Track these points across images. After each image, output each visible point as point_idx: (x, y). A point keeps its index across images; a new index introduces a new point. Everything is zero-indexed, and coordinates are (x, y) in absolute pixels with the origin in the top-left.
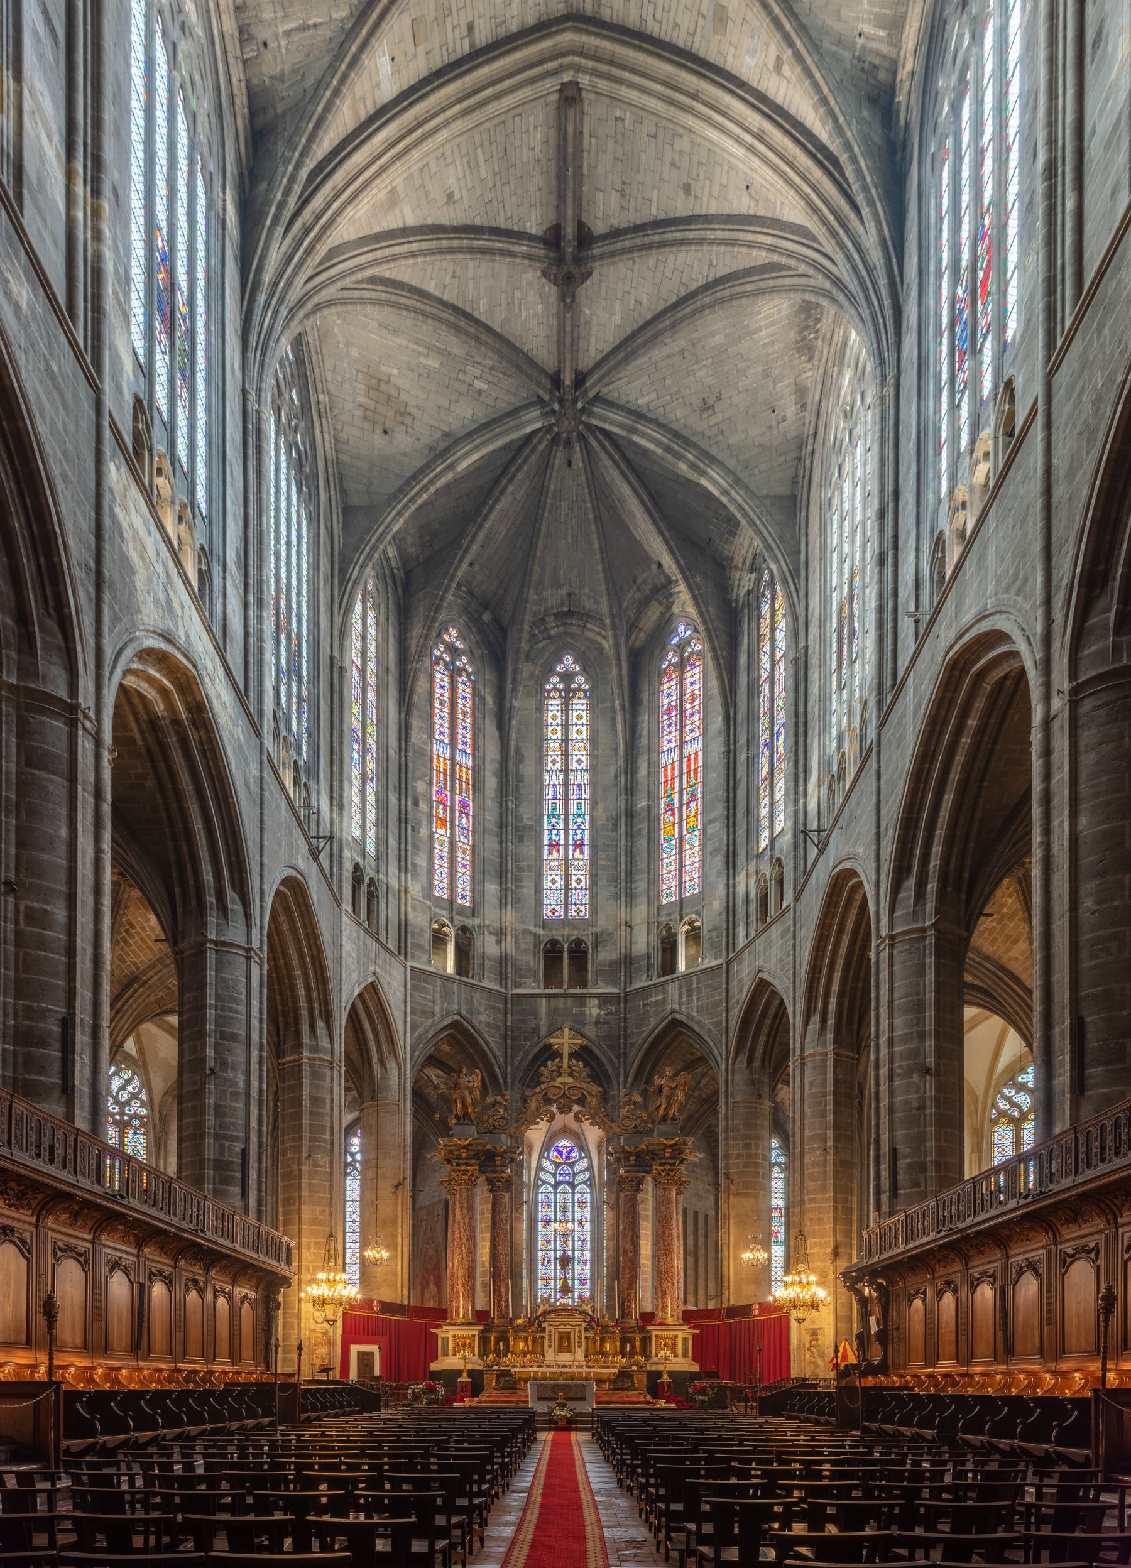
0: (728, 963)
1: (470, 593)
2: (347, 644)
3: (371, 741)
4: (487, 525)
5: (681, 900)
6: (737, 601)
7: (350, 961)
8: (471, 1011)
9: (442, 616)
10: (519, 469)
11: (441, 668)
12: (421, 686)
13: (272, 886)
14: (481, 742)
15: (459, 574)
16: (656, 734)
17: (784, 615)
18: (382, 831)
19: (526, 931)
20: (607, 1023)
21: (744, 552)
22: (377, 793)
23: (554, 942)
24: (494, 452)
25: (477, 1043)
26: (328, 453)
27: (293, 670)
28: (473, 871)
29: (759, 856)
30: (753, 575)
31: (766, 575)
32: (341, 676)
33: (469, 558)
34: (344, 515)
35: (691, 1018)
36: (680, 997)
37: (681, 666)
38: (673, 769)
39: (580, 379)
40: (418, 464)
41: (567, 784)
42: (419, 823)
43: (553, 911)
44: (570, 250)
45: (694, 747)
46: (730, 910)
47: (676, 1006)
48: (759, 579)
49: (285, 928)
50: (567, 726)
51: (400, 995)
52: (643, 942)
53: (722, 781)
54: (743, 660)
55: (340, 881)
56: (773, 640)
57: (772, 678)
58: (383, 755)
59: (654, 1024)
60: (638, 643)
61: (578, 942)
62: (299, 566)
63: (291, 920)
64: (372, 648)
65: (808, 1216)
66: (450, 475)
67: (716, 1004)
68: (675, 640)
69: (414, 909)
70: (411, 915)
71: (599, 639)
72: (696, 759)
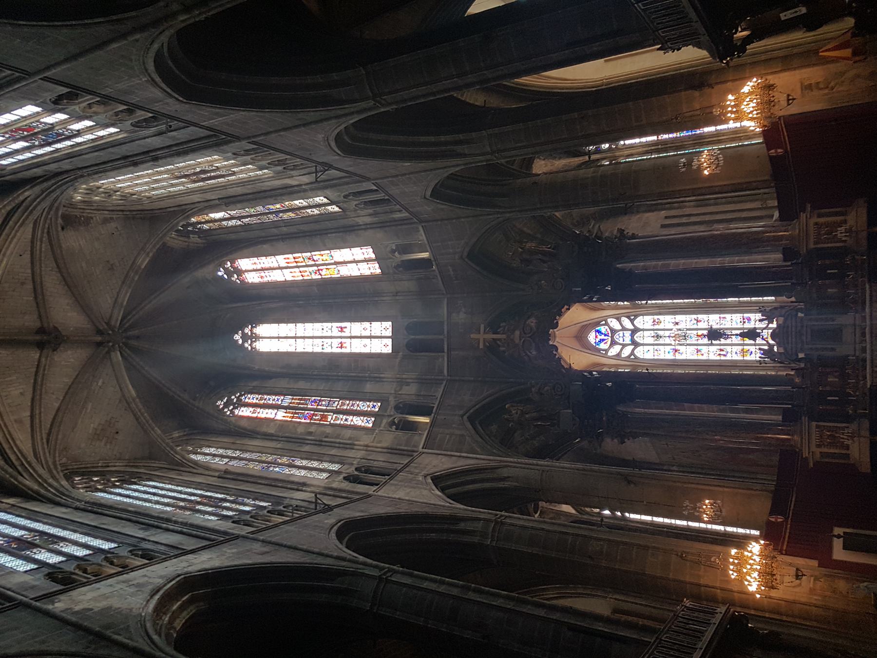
2: (214, 466)
3: (270, 458)
17: (207, 215)
22: (302, 459)
26: (124, 464)
39: (100, 332)
44: (45, 338)
46: (381, 225)
47: (457, 257)
57: (239, 218)
64: (221, 451)
66: (137, 400)
69: (380, 442)
70: (385, 445)
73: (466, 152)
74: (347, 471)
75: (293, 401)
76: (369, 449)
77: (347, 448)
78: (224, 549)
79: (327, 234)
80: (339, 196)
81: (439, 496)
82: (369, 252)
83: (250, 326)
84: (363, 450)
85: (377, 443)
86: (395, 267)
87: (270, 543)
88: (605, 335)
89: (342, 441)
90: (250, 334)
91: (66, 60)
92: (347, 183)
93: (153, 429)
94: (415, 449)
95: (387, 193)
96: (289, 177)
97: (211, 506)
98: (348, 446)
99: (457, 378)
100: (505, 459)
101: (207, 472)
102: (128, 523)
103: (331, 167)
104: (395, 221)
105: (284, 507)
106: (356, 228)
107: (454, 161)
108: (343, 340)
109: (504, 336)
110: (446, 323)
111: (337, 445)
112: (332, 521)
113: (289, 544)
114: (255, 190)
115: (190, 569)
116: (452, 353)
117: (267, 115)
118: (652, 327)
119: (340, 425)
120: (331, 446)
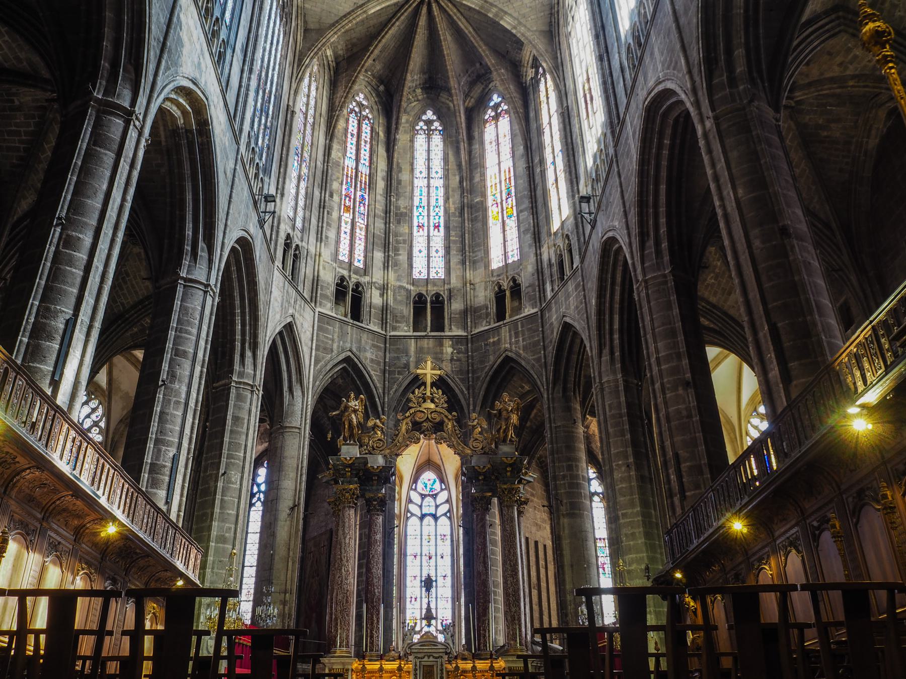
0: (542, 311)
1: (373, 75)
3: (306, 155)
4: (384, 41)
5: (507, 265)
6: (526, 83)
7: (276, 304)
8: (359, 349)
9: (356, 87)
10: (403, 14)
11: (354, 114)
12: (341, 124)
13: (230, 243)
14: (375, 159)
15: (367, 64)
16: (482, 156)
18: (308, 214)
19: (401, 287)
20: (459, 360)
21: (527, 58)
23: (420, 295)
24: (388, 6)
25: (363, 376)
27: (264, 110)
28: (366, 243)
29: (555, 234)
30: (534, 70)
31: (541, 70)
32: (292, 116)
33: (373, 57)
34: (304, 33)
35: (519, 355)
36: (510, 339)
37: (496, 118)
38: (496, 178)
40: (348, 10)
41: (429, 187)
42: (332, 208)
43: (420, 273)
45: (507, 163)
46: (539, 271)
47: (508, 346)
48: (537, 73)
49: (234, 276)
50: (429, 151)
51: (309, 334)
52: (483, 296)
53: (527, 185)
54: (532, 114)
55: (276, 245)
56: (548, 103)
57: (550, 124)
58: (313, 164)
59: (493, 360)
60: (470, 104)
61: (437, 295)
62: (276, 56)
63: (239, 270)
64: (312, 102)
65: (624, 531)
66: (365, 16)
67: (536, 344)
68: (492, 104)
69: (324, 268)
71: (448, 102)
72: (509, 171)
73: (603, 359)
74: (295, 237)
75: (364, 176)
76: (317, 257)
77: (317, 234)
78: (228, 134)
79: (533, 214)
80: (568, 230)
81: (274, 331)
82: (514, 256)
83: (440, 128)
84: (316, 251)
85: (323, 265)
86: (498, 283)
87: (234, 176)
88: (431, 489)
89: (324, 229)
90: (433, 128)
91: (674, 11)
92: (579, 240)
93: (335, 33)
94: (318, 304)
95: (569, 279)
96: (586, 182)
97: (262, 105)
98: (319, 236)
99: (388, 345)
100: (310, 393)
101: (292, 92)
102: (247, 30)
103: (593, 227)
104: (543, 285)
105: (262, 178)
106: (538, 244)
107: (595, 344)
108: (426, 228)
109: (428, 394)
110: (442, 334)
111: (320, 225)
112: (252, 230)
113: (234, 195)
114: (575, 146)
115: (212, 107)
116: (413, 340)
117: (633, 178)
118: (438, 534)
119: (339, 227)
120: (319, 218)
